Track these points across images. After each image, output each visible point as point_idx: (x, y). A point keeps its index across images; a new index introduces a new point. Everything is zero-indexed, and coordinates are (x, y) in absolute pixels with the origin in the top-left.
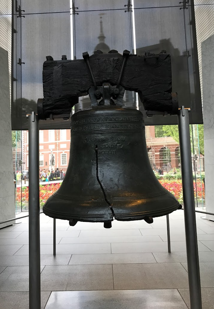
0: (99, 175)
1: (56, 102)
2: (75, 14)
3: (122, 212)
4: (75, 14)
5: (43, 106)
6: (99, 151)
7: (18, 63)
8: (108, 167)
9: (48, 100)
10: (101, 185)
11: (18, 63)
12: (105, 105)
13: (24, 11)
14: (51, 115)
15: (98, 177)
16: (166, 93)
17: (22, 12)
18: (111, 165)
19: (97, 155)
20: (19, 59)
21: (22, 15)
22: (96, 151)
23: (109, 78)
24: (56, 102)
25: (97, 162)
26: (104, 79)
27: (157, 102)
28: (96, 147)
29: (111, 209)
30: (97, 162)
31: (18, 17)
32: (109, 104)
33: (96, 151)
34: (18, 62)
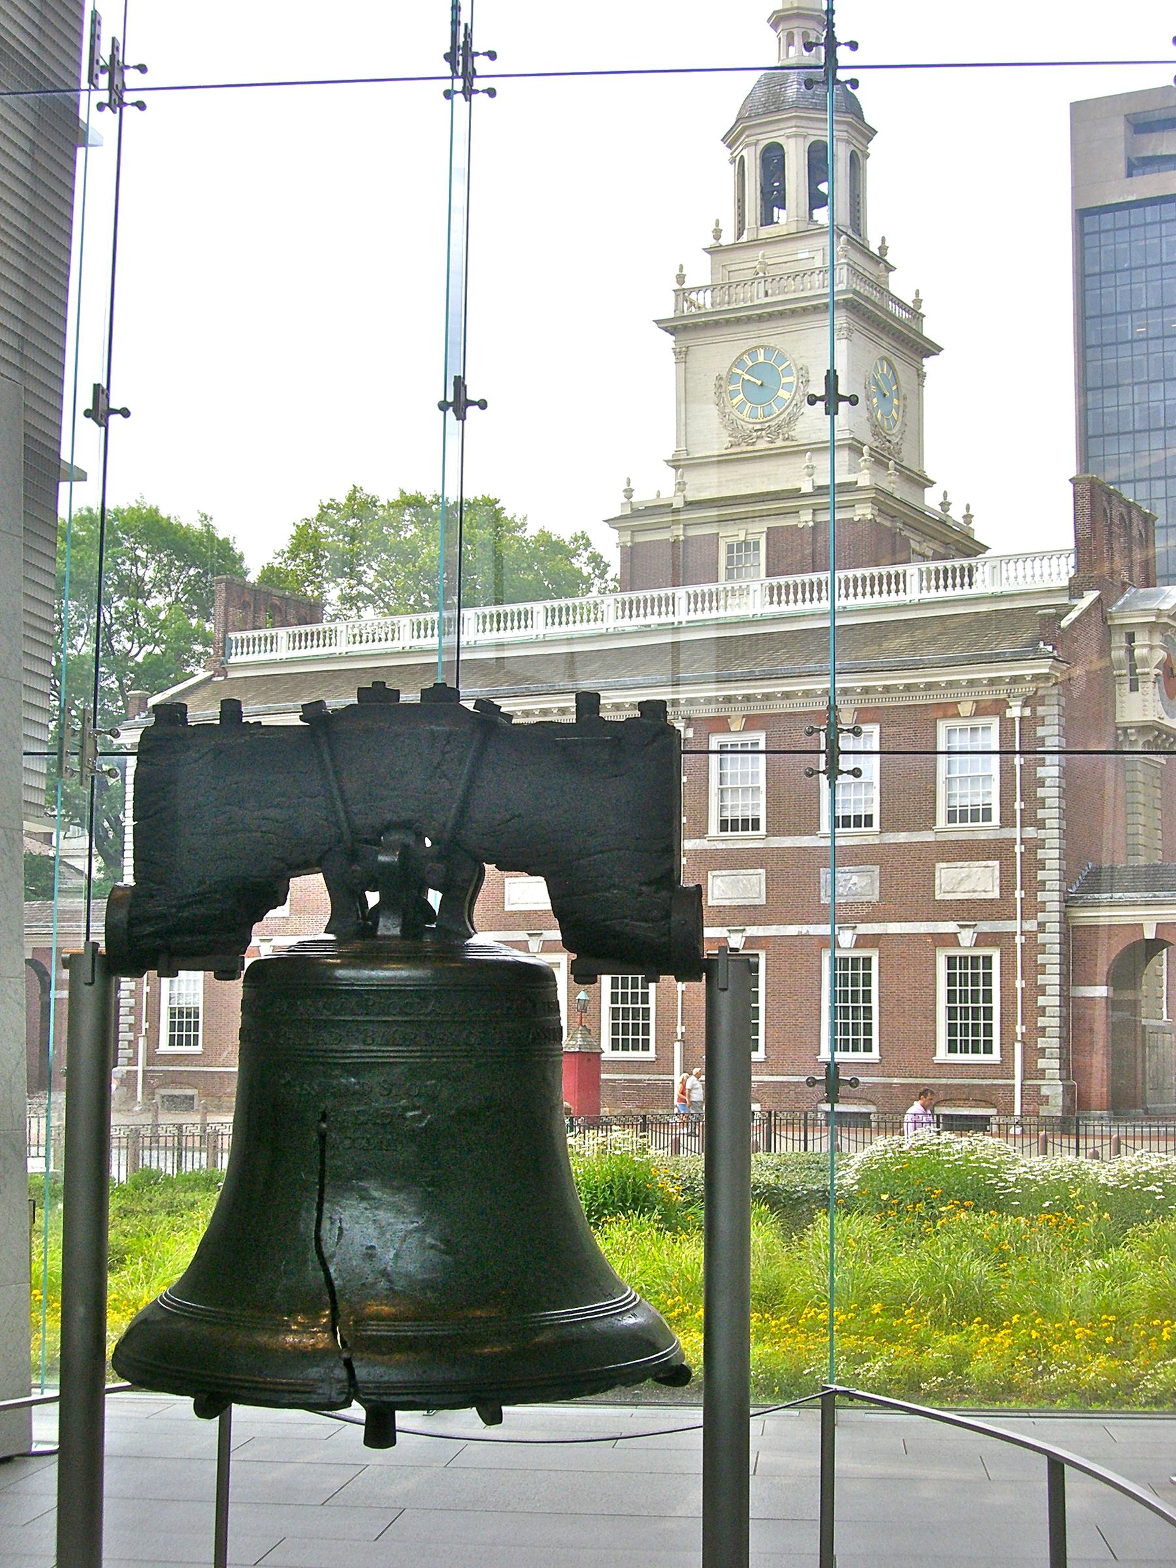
0: (325, 1234)
1: (181, 908)
2: (477, 92)
3: (386, 1378)
4: (477, 92)
5: (133, 922)
6: (333, 1136)
7: (87, 414)
8: (363, 1205)
9: (152, 897)
10: (326, 1271)
11: (87, 414)
12: (385, 937)
13: (142, 69)
14: (163, 959)
15: (318, 1239)
16: (643, 888)
17: (132, 78)
18: (376, 1194)
19: (323, 1152)
20: (97, 387)
21: (128, 97)
22: (323, 1137)
23: (405, 815)
24: (181, 908)
25: (322, 1178)
26: (388, 816)
27: (607, 926)
28: (324, 1118)
29: (348, 1364)
30: (322, 1178)
31: (100, 107)
32: (397, 931)
33: (323, 1137)
34: (90, 405)
